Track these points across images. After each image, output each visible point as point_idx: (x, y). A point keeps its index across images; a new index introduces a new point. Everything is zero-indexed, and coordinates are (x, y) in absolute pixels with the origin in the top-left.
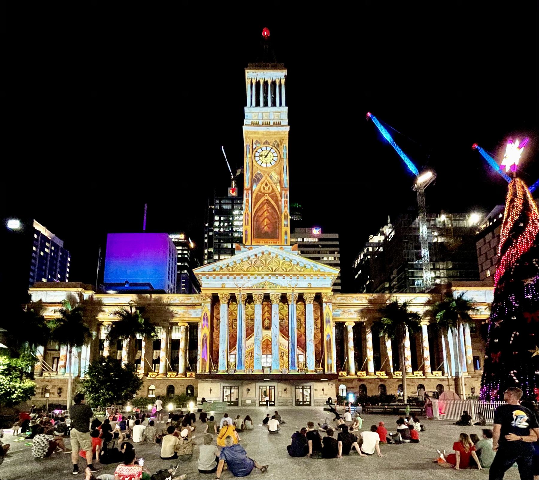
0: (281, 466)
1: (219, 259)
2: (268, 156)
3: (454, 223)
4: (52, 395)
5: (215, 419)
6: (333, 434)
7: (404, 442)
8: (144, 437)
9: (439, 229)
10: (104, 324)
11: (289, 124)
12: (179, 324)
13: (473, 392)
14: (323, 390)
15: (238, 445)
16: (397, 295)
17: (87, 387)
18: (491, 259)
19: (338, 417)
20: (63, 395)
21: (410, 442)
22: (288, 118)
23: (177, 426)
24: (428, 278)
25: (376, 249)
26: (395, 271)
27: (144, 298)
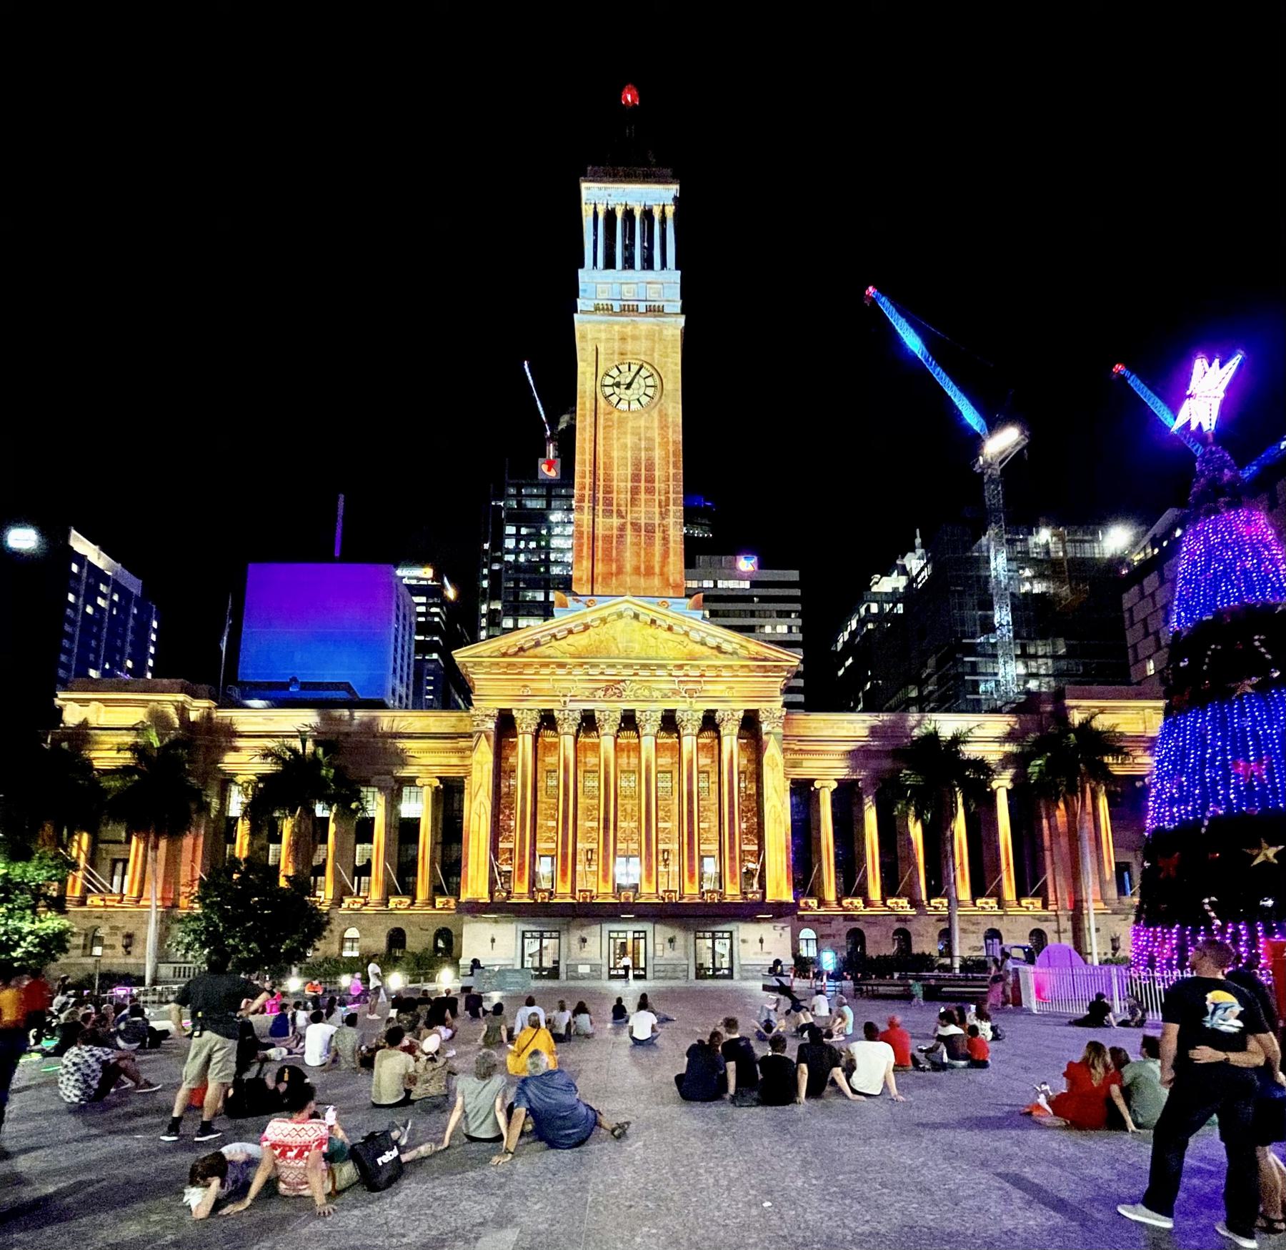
0: (659, 1125)
1: (516, 628)
3: (1069, 549)
4: (108, 951)
5: (504, 1012)
6: (785, 1047)
7: (953, 1067)
8: (333, 1053)
9: (1035, 563)
10: (240, 779)
11: (683, 312)
12: (418, 782)
13: (1115, 949)
14: (761, 941)
15: (560, 1071)
16: (935, 716)
17: (194, 931)
18: (1156, 633)
19: (797, 1006)
20: (136, 950)
21: (969, 1066)
22: (682, 297)
23: (412, 1027)
24: (1009, 678)
25: (887, 607)
26: (932, 662)
27: (331, 719)
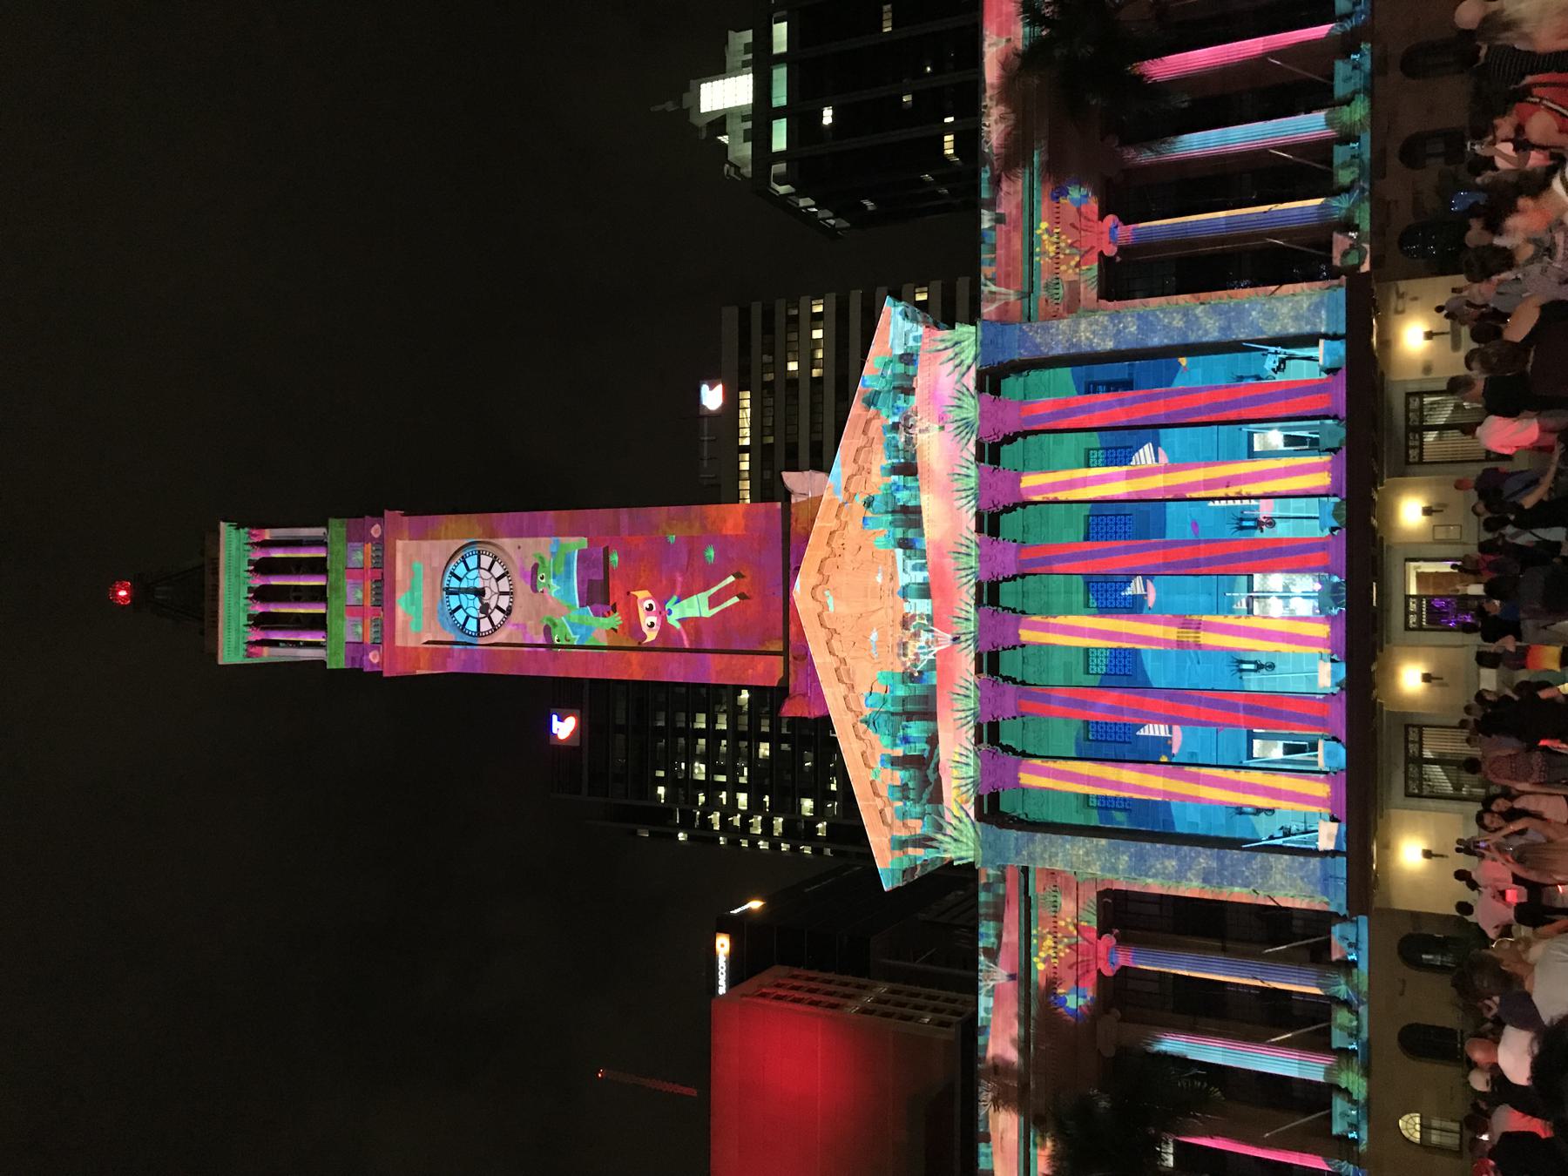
2: (479, 584)
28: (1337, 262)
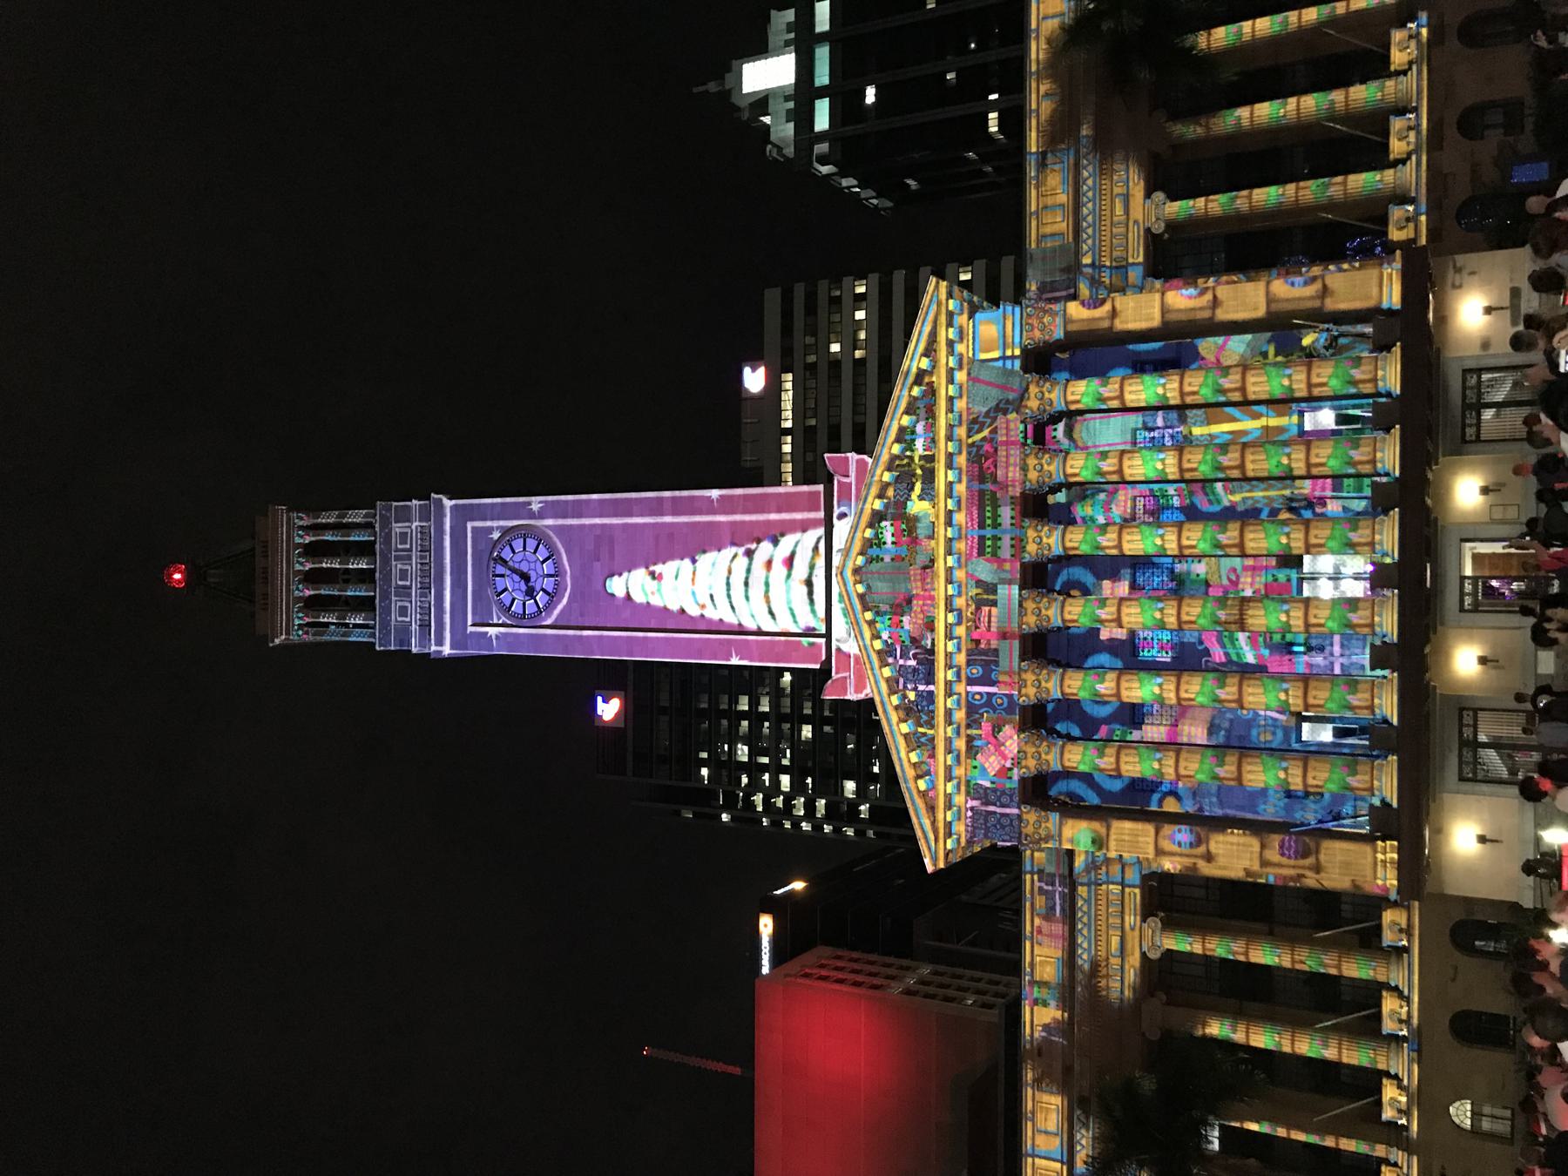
28: (1395, 235)
